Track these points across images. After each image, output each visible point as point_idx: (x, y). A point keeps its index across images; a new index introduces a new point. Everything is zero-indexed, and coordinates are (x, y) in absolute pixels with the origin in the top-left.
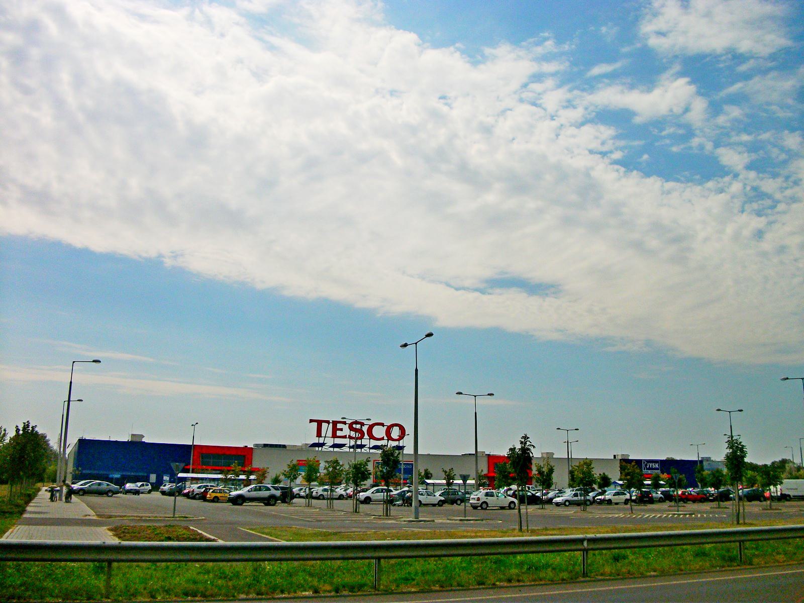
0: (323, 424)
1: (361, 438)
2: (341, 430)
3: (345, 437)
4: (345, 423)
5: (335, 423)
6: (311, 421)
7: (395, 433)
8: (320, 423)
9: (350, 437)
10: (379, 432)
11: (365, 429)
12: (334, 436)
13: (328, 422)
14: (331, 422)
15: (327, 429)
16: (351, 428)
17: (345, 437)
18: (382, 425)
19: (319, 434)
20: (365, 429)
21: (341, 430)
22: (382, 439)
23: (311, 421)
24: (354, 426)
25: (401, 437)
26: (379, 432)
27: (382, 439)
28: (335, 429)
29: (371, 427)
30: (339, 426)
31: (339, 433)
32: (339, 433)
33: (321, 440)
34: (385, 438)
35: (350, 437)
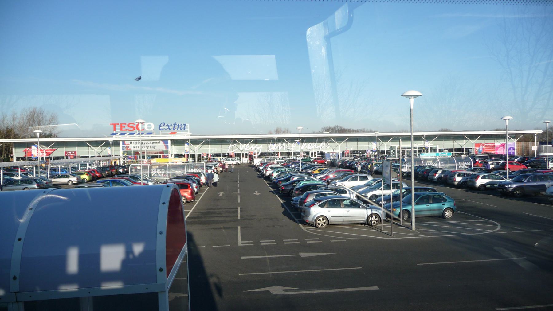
0: (116, 125)
1: (134, 129)
2: (124, 127)
3: (126, 130)
4: (126, 124)
5: (121, 125)
8: (115, 125)
9: (128, 130)
12: (121, 130)
13: (118, 124)
14: (119, 124)
15: (118, 127)
16: (129, 126)
19: (115, 129)
24: (130, 125)
28: (122, 127)
31: (123, 129)
32: (123, 129)
33: (115, 132)
35: (128, 130)
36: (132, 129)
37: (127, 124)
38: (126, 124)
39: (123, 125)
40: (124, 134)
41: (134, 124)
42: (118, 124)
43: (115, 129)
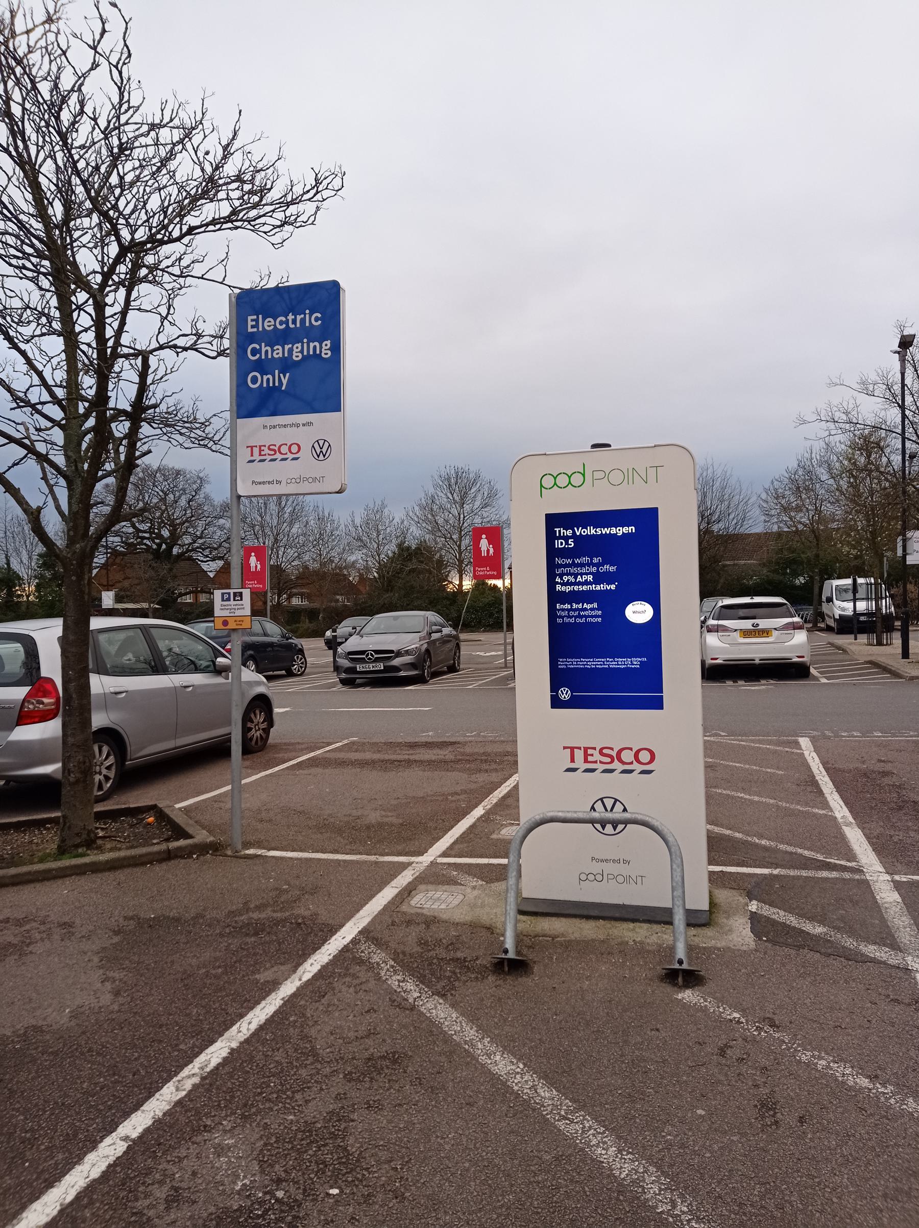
1: (612, 761)
2: (592, 755)
3: (596, 762)
4: (594, 749)
5: (586, 749)
6: (565, 748)
7: (645, 756)
8: (572, 749)
9: (601, 762)
10: (627, 756)
11: (614, 754)
12: (586, 761)
13: (579, 748)
15: (579, 755)
16: (601, 753)
17: (596, 762)
18: (631, 749)
19: (573, 760)
20: (614, 754)
21: (592, 755)
22: (632, 763)
23: (565, 748)
24: (605, 751)
25: (652, 760)
26: (627, 756)
27: (632, 763)
28: (586, 755)
29: (619, 753)
30: (590, 752)
32: (590, 759)
34: (634, 761)
35: (601, 762)
36: (609, 760)
37: (598, 749)
38: (594, 749)
39: (590, 752)
40: (593, 770)
41: (612, 749)
42: (579, 748)
43: (573, 760)
